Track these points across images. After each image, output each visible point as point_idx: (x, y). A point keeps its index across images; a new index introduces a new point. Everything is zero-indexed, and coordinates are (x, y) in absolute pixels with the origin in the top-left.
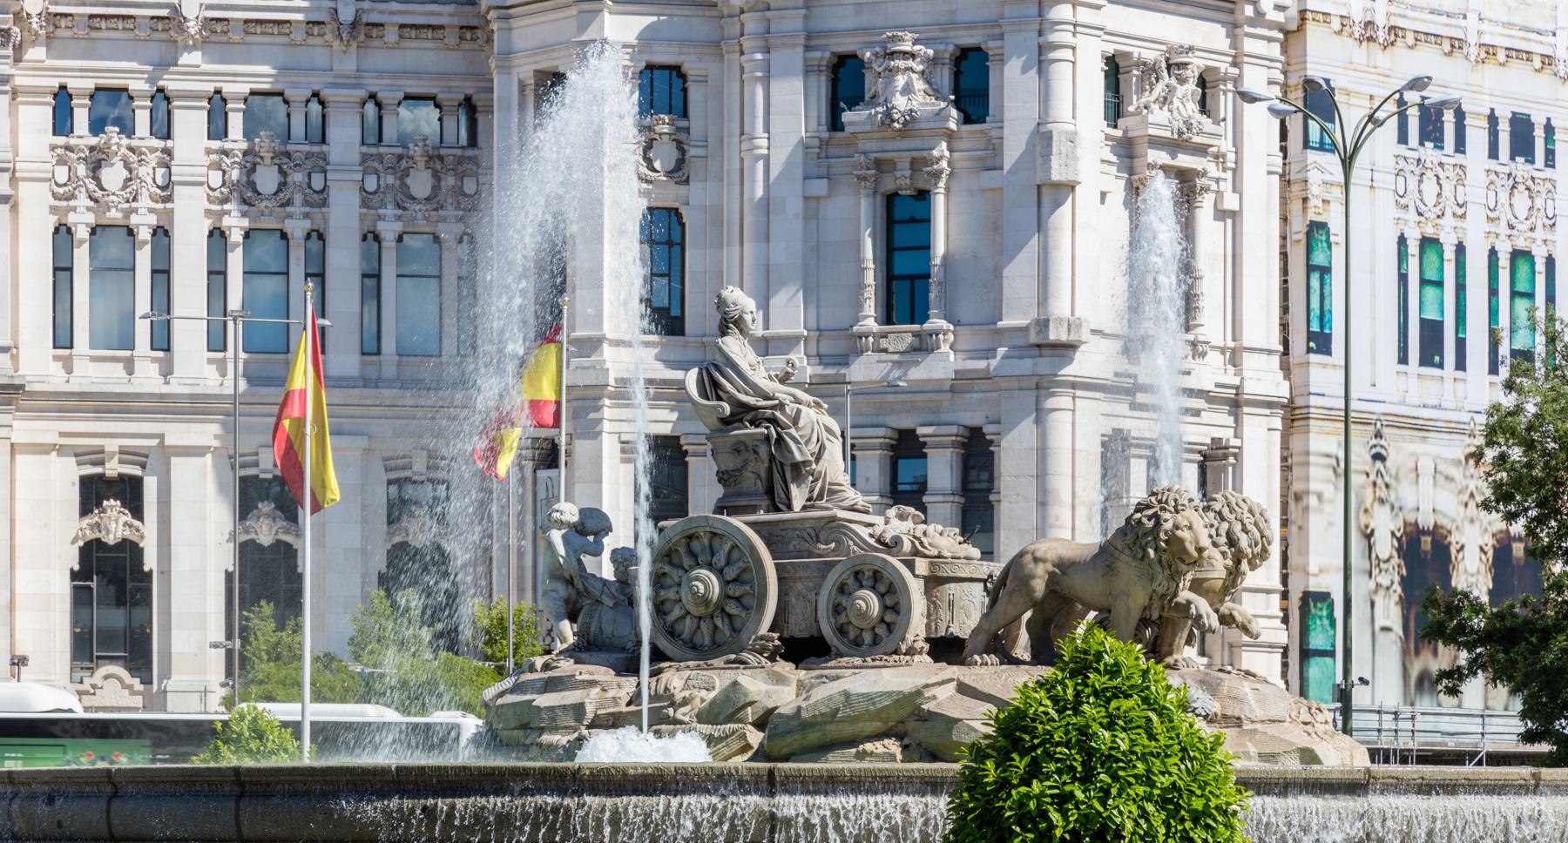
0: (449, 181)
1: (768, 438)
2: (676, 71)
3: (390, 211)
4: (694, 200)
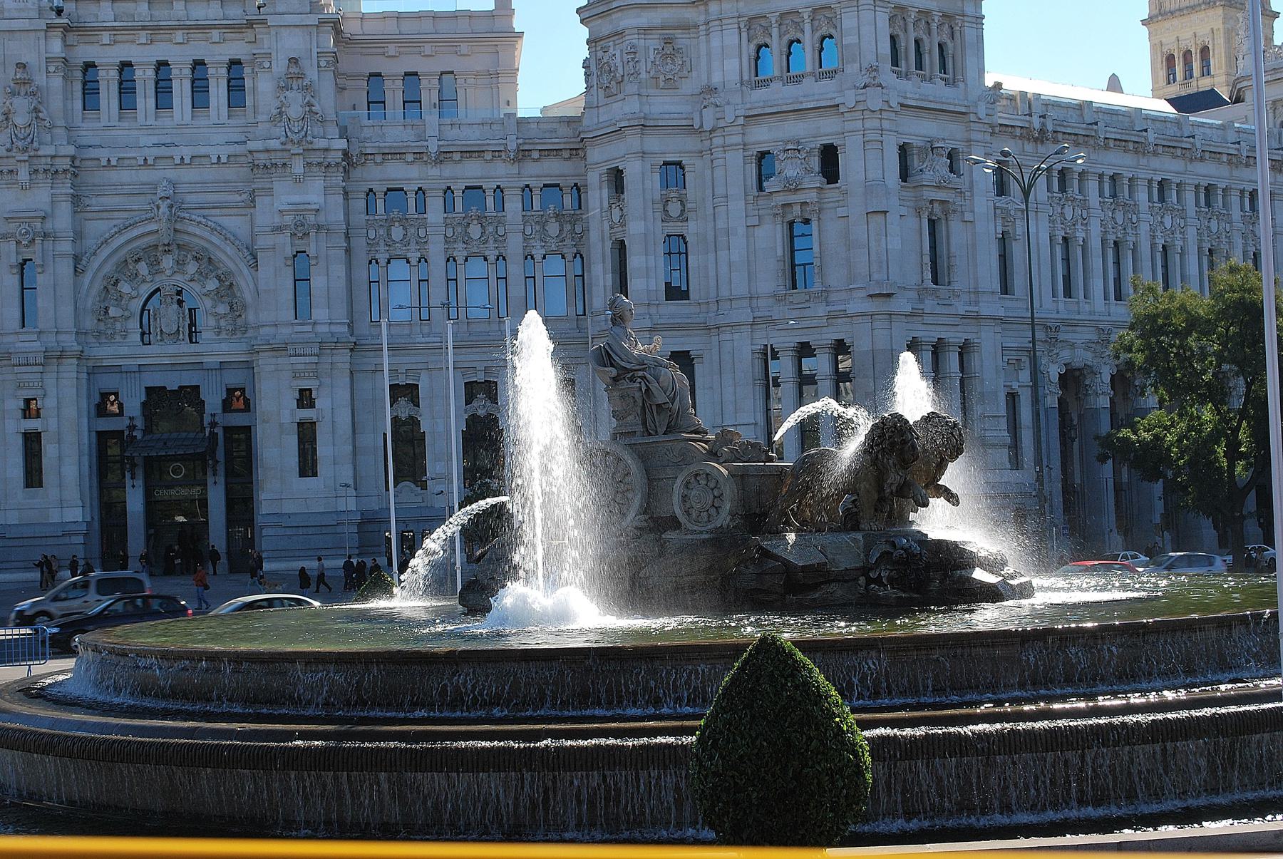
0: (568, 227)
1: (640, 389)
2: (679, 164)
3: (539, 243)
4: (692, 229)
